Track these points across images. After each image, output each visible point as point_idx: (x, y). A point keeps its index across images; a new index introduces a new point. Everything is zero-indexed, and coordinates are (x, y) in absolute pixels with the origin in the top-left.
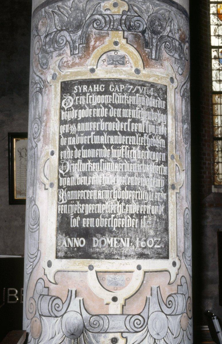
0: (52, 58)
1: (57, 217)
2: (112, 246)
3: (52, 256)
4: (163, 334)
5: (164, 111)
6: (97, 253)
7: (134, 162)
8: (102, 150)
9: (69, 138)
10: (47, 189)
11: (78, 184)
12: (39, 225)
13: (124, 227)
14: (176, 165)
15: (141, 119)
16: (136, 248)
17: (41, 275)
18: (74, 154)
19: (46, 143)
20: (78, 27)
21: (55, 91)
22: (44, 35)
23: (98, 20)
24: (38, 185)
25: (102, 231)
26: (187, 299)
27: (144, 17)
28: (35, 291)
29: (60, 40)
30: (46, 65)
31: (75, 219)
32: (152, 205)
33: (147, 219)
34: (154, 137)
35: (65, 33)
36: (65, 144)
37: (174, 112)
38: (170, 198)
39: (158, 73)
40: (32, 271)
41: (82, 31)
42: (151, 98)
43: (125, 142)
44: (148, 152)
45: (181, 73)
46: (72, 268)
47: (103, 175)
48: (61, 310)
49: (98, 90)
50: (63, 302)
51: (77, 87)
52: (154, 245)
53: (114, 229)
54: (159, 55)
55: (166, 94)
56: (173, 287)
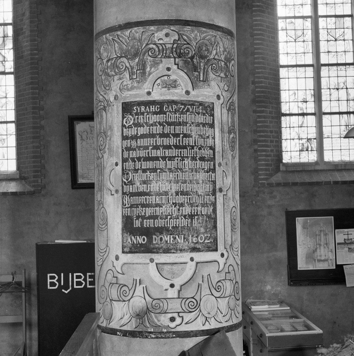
0: (114, 81)
1: (122, 219)
2: (169, 242)
3: (119, 252)
4: (213, 313)
5: (212, 126)
6: (156, 249)
7: (186, 171)
8: (159, 162)
9: (130, 152)
10: (113, 195)
11: (139, 191)
12: (107, 225)
13: (179, 226)
14: (223, 171)
15: (191, 134)
16: (189, 244)
17: (111, 267)
18: (135, 166)
19: (111, 155)
20: (136, 55)
21: (117, 110)
22: (106, 60)
23: (153, 48)
24: (105, 191)
25: (161, 230)
26: (234, 284)
27: (192, 44)
28: (106, 280)
29: (120, 66)
30: (109, 87)
31: (137, 221)
32: (202, 207)
33: (198, 219)
34: (203, 149)
35: (124, 60)
36: (127, 157)
37: (220, 125)
38: (218, 200)
39: (205, 93)
40: (103, 263)
41: (139, 59)
42: (200, 116)
43: (178, 155)
44: (198, 162)
45: (226, 89)
46: (135, 261)
47: (160, 183)
48: (128, 295)
49: (154, 111)
50: (130, 289)
51: (136, 107)
52: (205, 240)
53: (171, 228)
54: (206, 77)
55: (213, 111)
56: (222, 274)
